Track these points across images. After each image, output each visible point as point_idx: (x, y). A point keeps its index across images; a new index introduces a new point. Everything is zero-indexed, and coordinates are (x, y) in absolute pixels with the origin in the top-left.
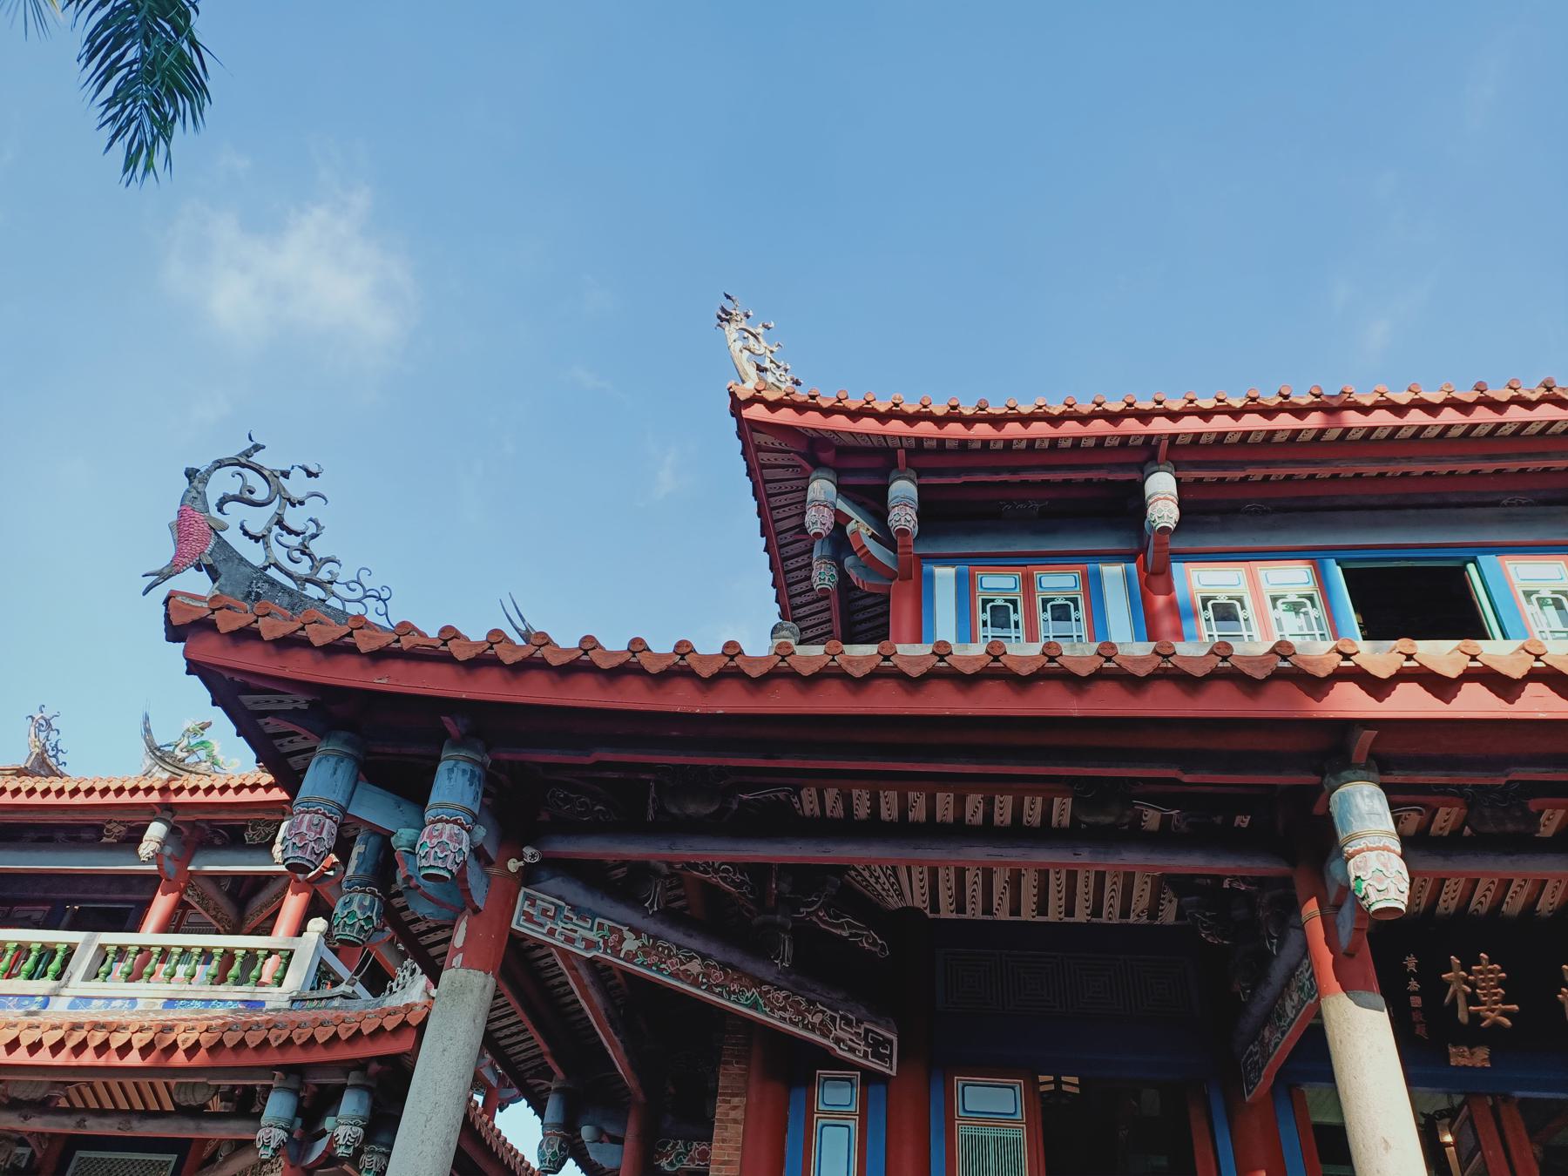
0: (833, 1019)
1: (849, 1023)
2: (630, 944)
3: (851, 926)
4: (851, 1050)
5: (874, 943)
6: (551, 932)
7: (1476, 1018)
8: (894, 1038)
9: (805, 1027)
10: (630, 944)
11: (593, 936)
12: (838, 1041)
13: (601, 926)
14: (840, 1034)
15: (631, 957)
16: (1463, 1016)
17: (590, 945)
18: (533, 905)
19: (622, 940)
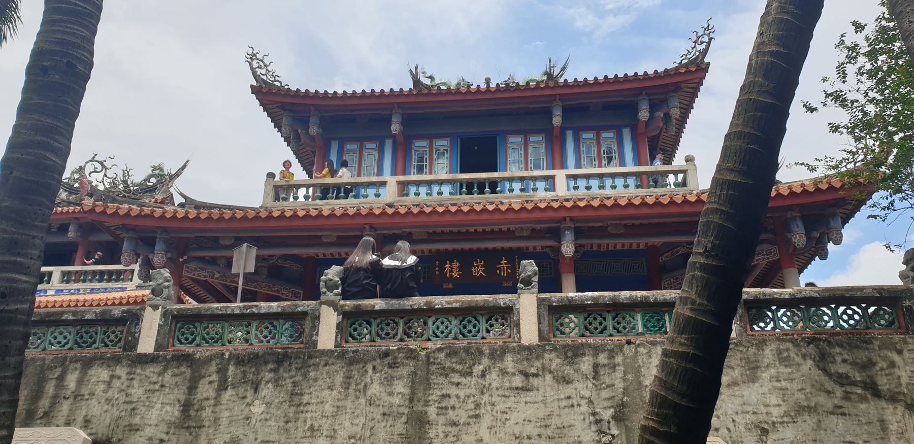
0: (281, 289)
1: (286, 289)
2: (217, 275)
3: (290, 263)
4: (287, 296)
5: (298, 267)
6: (194, 275)
7: (451, 276)
8: (302, 292)
9: (272, 291)
10: (217, 275)
11: (206, 274)
12: (282, 294)
13: (208, 272)
14: (283, 292)
15: (217, 279)
16: (448, 275)
17: (205, 276)
18: (188, 268)
19: (214, 274)
